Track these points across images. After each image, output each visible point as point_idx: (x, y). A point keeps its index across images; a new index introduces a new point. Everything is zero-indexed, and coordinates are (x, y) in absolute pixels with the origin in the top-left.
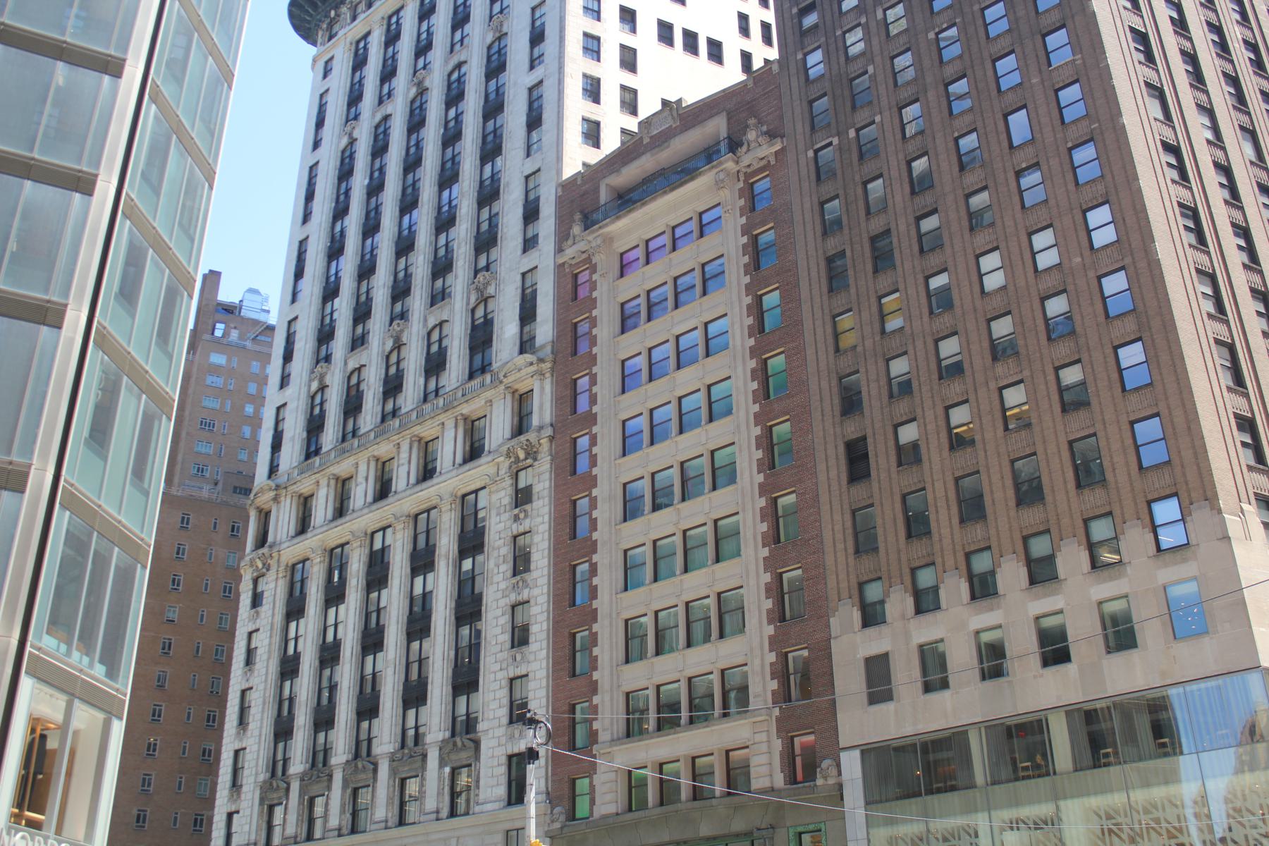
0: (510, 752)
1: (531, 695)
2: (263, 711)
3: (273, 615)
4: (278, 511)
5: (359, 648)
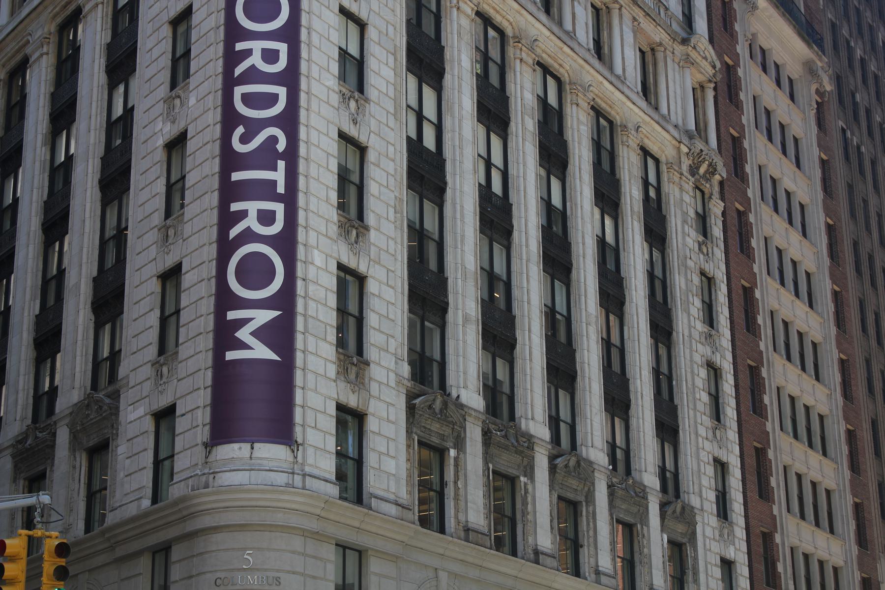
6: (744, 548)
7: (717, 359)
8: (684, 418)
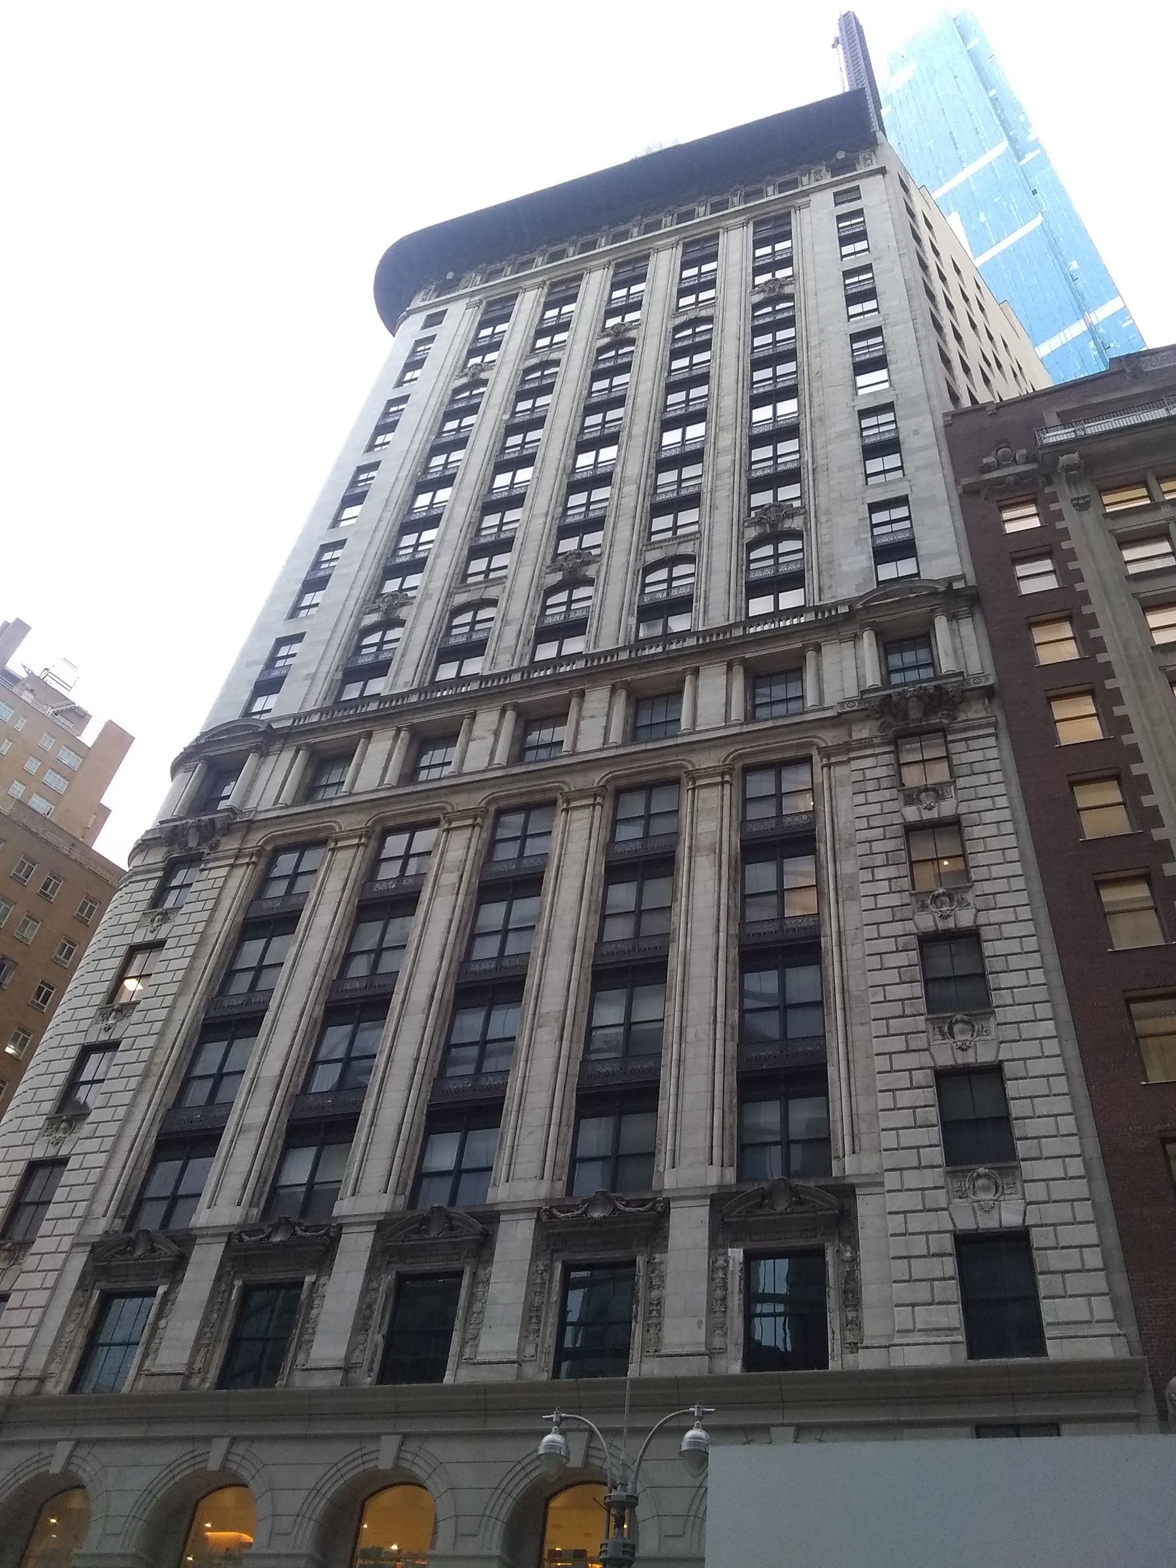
0: (966, 1223)
1: (1017, 1108)
2: (138, 1091)
3: (209, 921)
4: (258, 767)
5: (450, 990)
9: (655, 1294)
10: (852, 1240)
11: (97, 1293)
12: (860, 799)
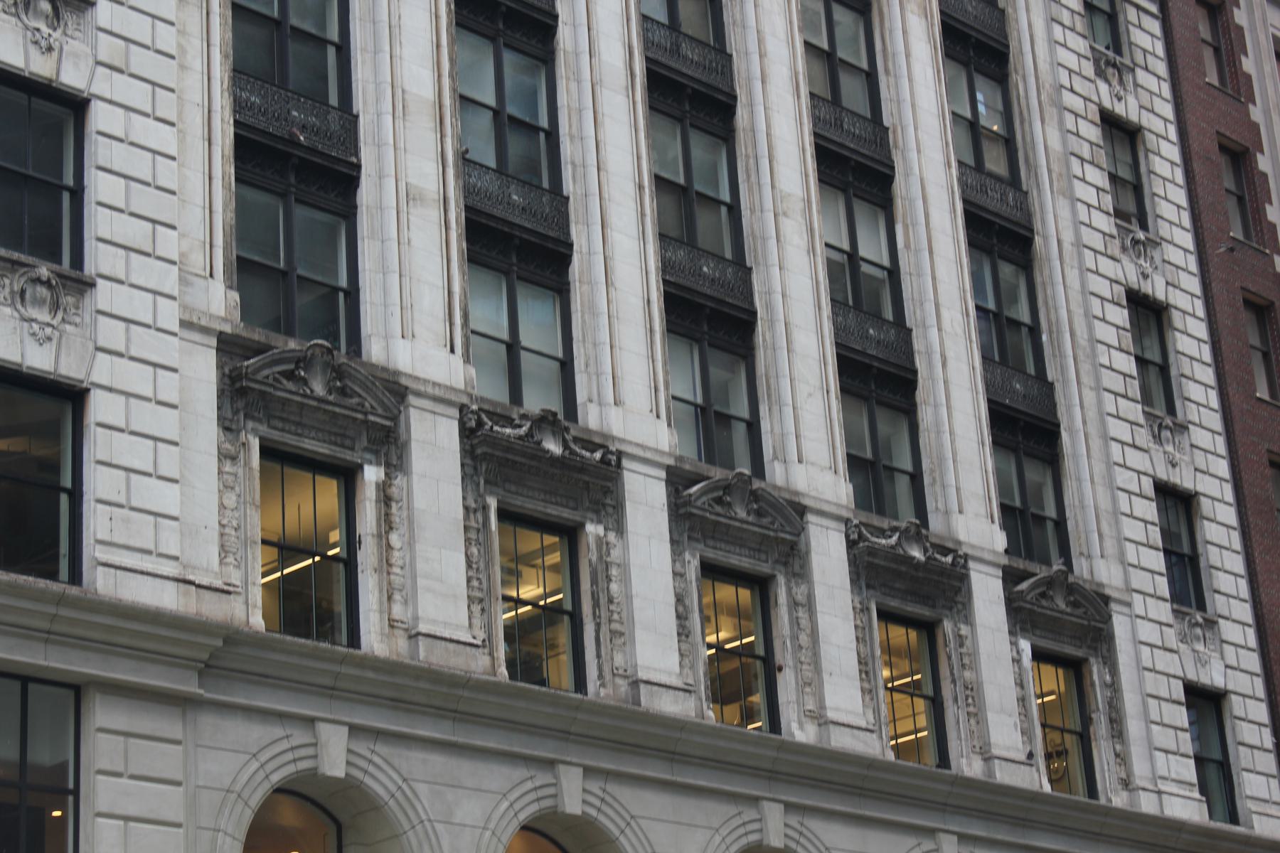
6: (1253, 661)
7: (1157, 289)
8: (1069, 408)
9: (967, 674)
10: (1110, 662)
11: (255, 444)
12: (1058, 31)
